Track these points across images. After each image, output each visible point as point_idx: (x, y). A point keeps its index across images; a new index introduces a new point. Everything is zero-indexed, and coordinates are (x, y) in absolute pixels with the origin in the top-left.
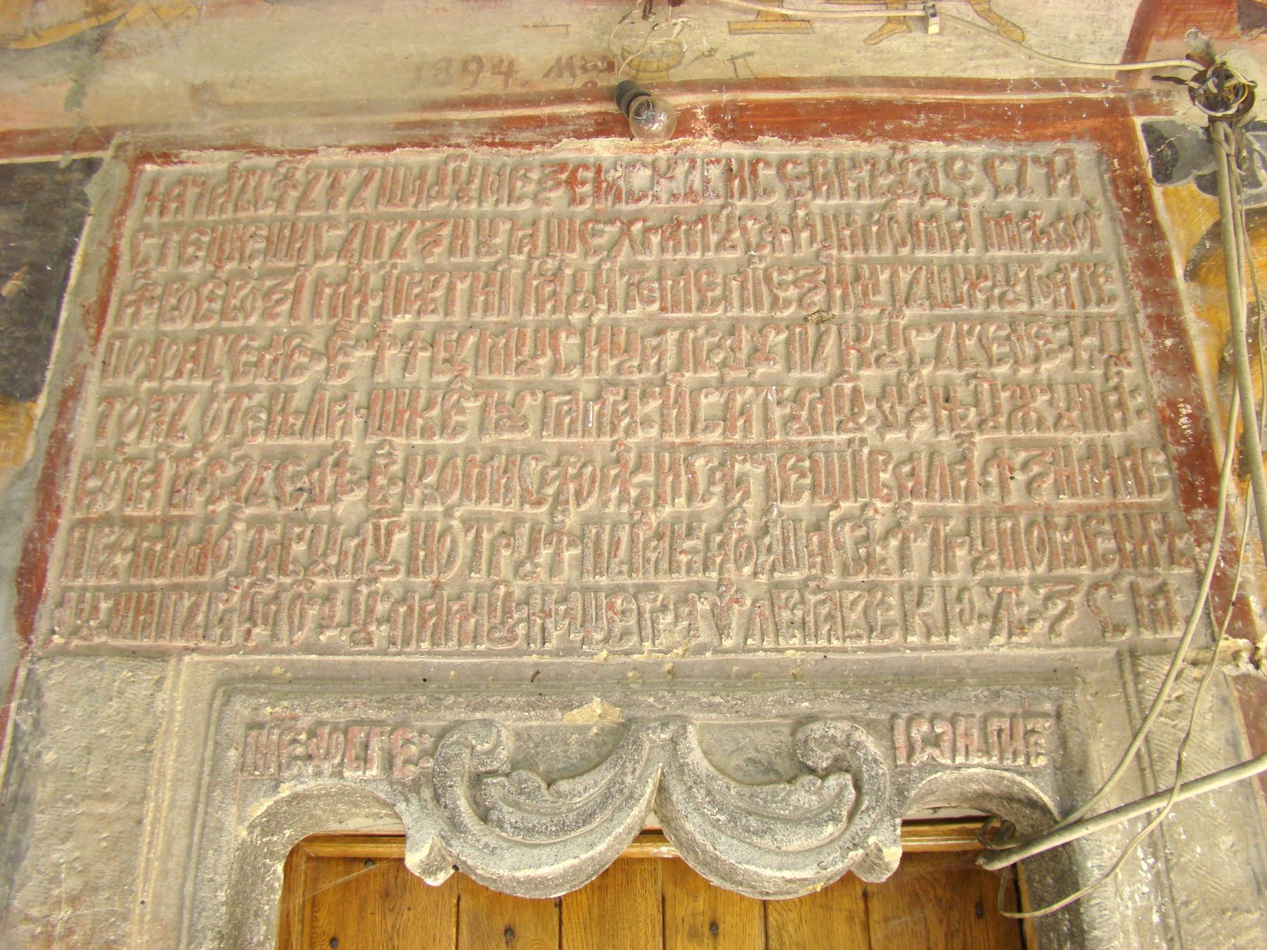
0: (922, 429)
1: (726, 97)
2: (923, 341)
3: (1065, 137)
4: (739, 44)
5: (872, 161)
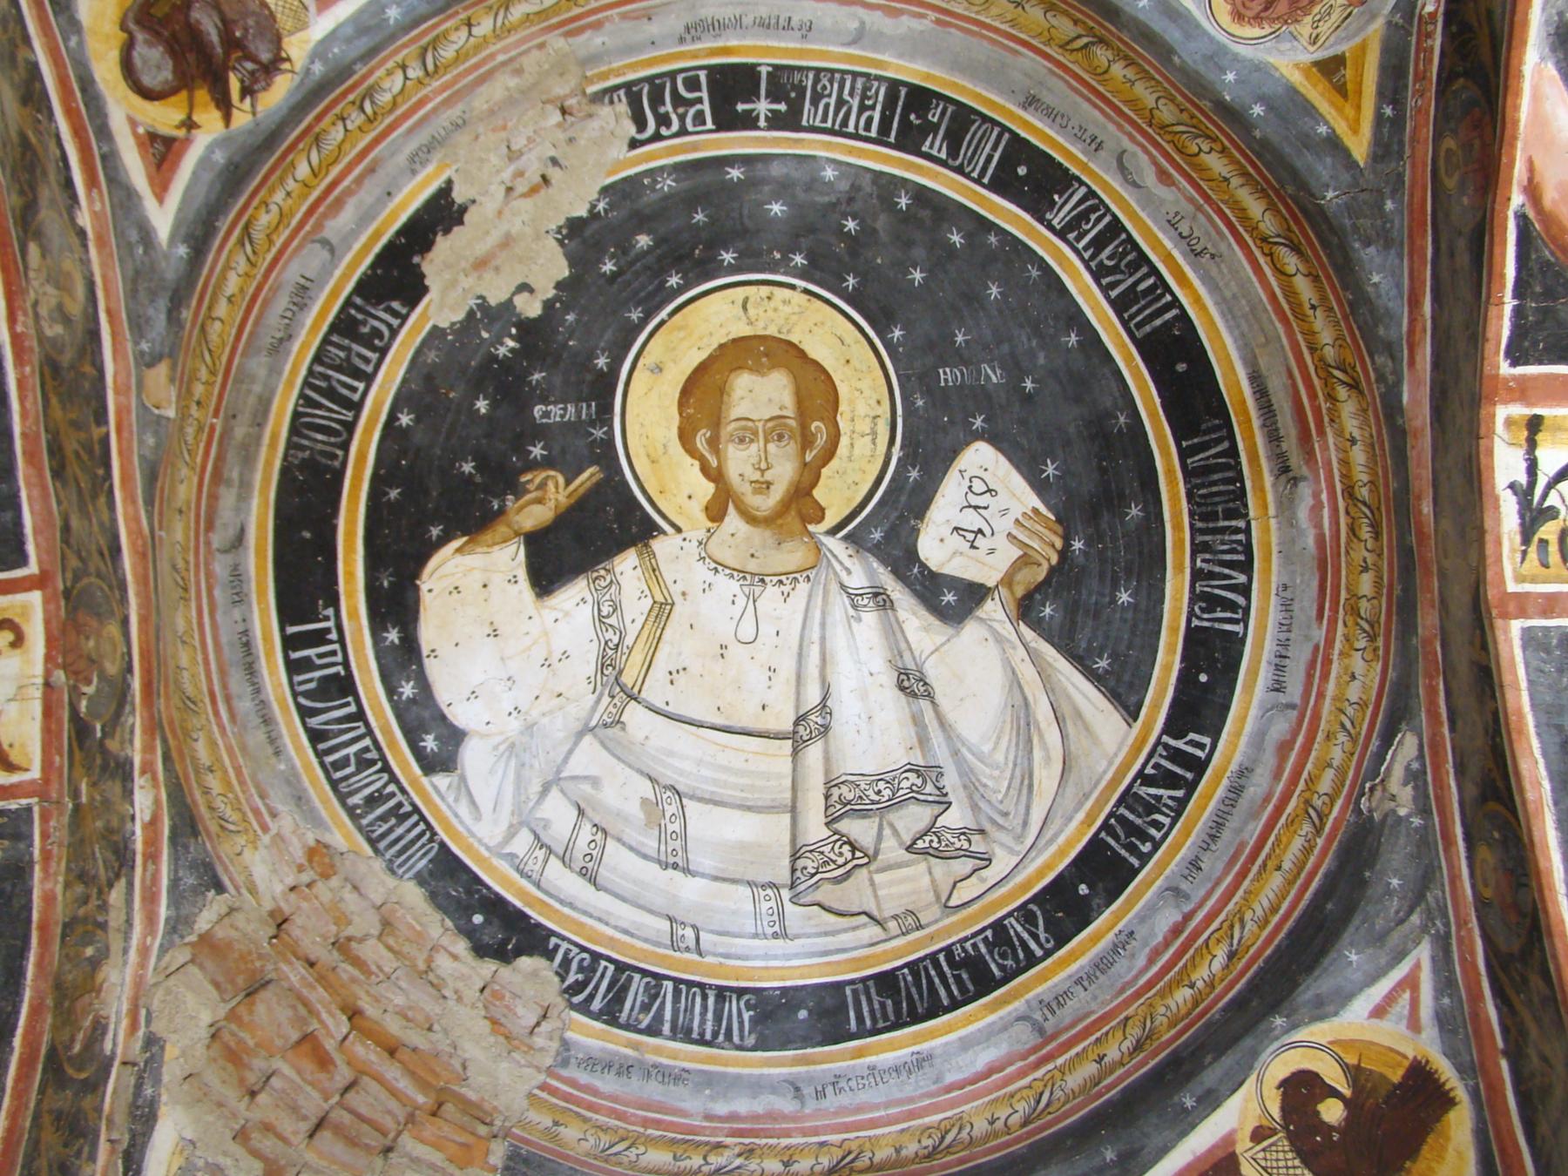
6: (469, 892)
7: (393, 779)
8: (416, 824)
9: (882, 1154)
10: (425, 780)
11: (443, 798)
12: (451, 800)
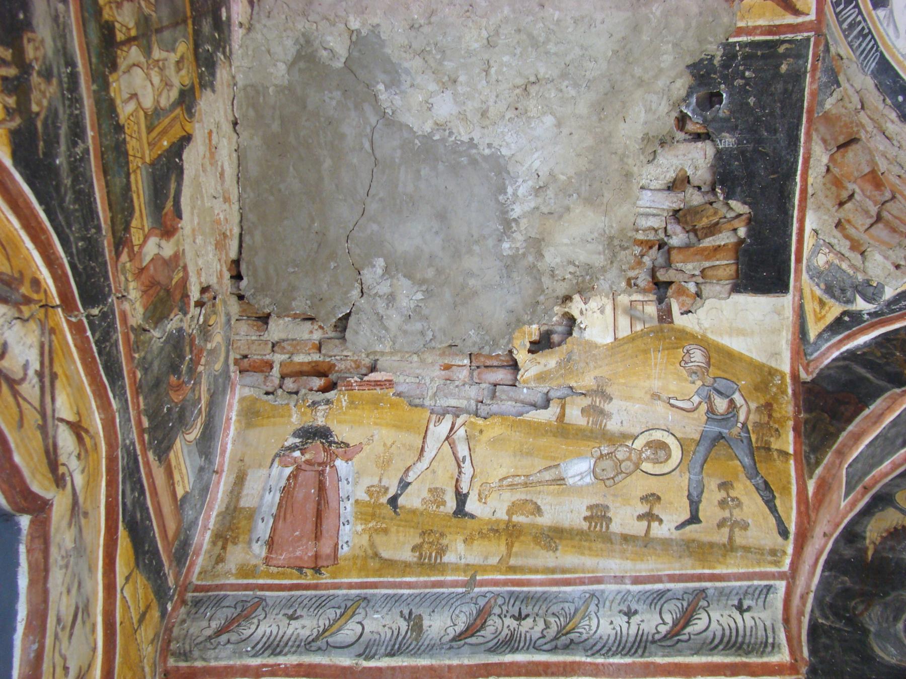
6: (895, 82)
7: (860, 13)
8: (870, 41)
10: (873, 12)
11: (881, 24)
12: (885, 25)
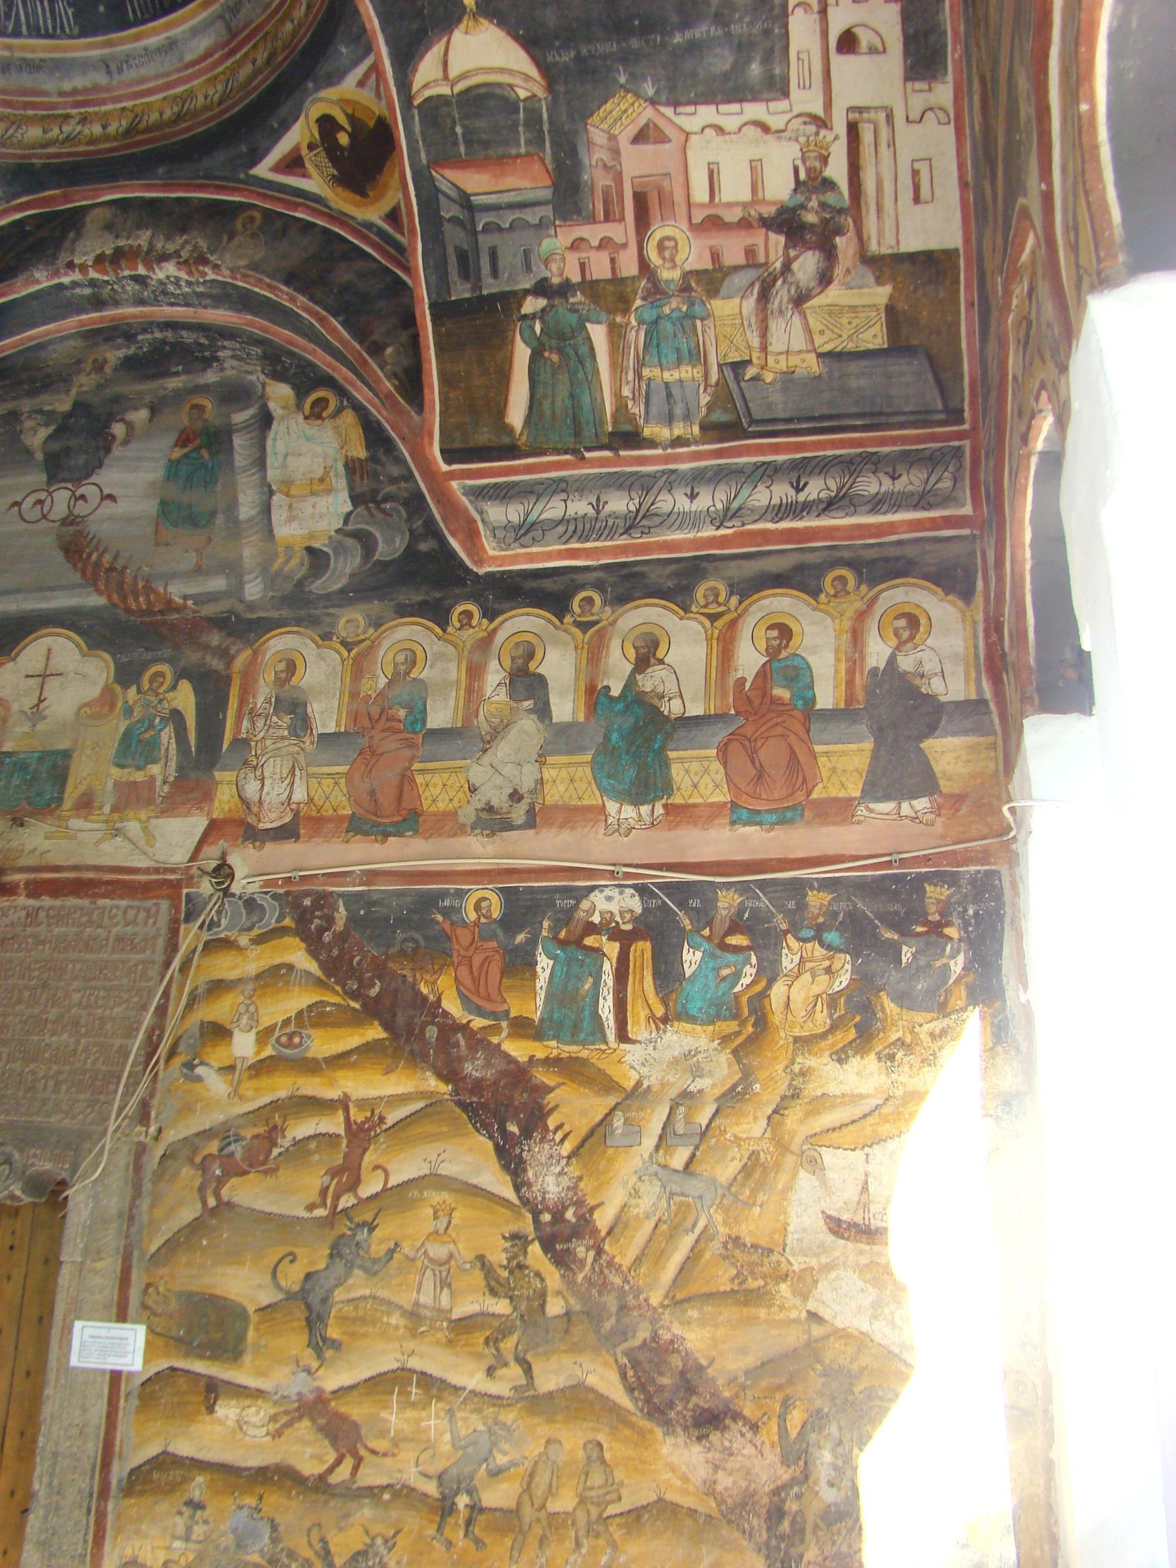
0: (65, 1035)
1: (33, 876)
2: (76, 997)
3: (157, 897)
4: (47, 845)
5: (82, 909)
9: (154, 117)
